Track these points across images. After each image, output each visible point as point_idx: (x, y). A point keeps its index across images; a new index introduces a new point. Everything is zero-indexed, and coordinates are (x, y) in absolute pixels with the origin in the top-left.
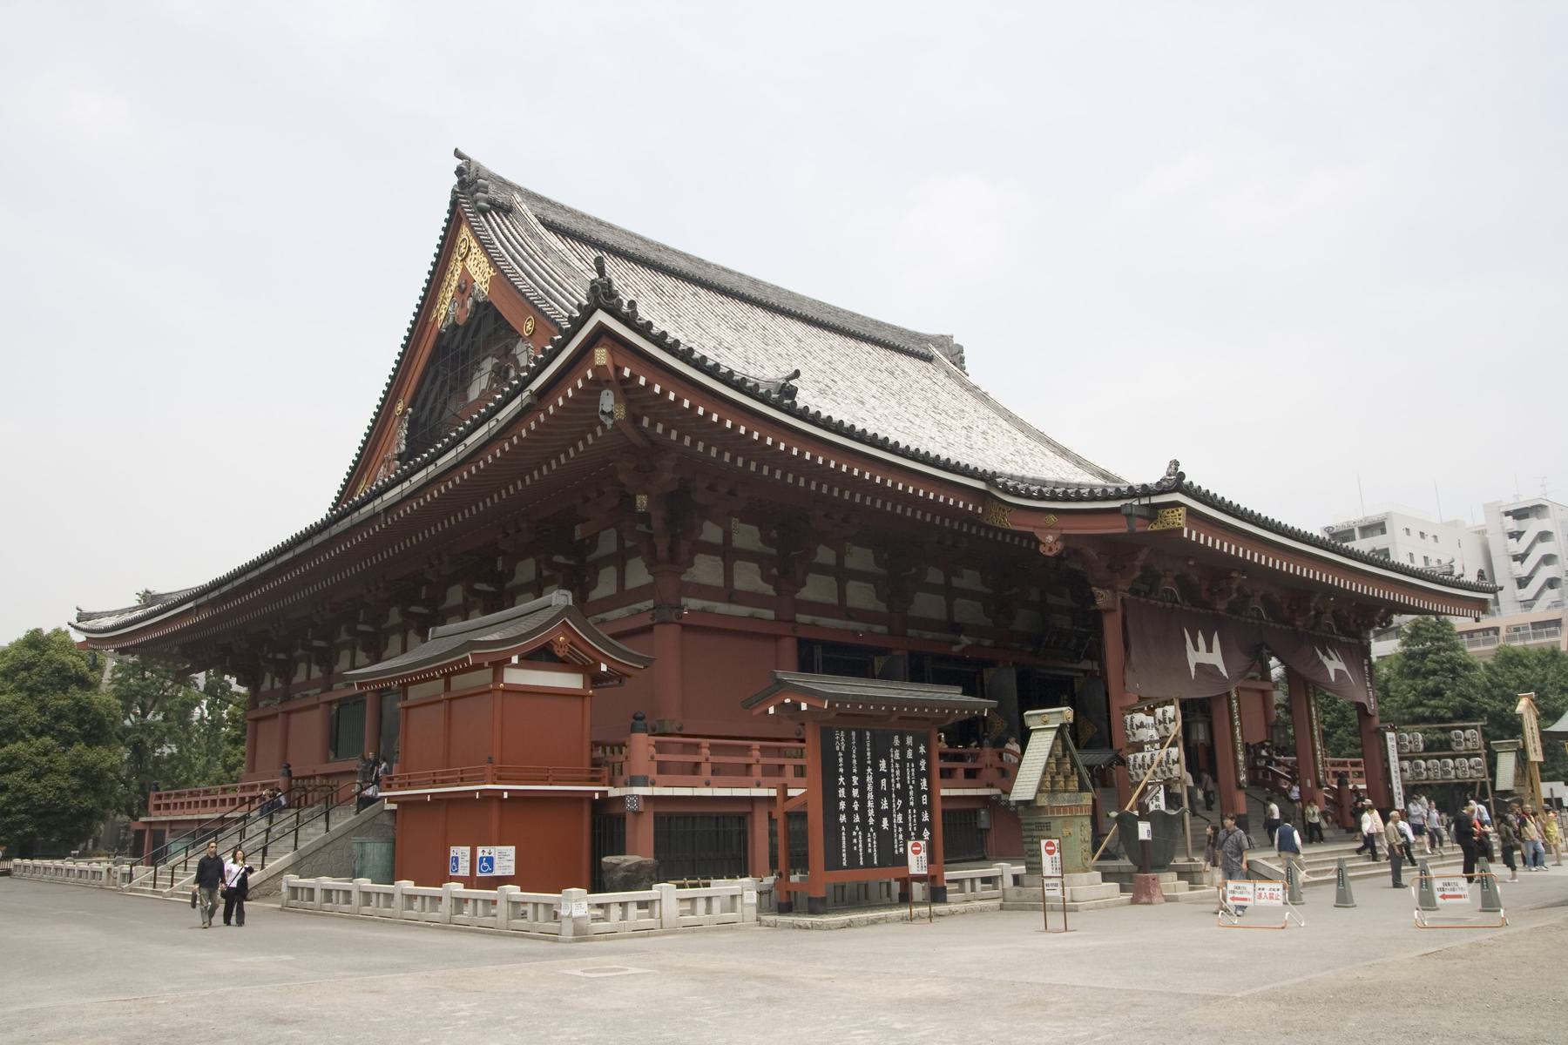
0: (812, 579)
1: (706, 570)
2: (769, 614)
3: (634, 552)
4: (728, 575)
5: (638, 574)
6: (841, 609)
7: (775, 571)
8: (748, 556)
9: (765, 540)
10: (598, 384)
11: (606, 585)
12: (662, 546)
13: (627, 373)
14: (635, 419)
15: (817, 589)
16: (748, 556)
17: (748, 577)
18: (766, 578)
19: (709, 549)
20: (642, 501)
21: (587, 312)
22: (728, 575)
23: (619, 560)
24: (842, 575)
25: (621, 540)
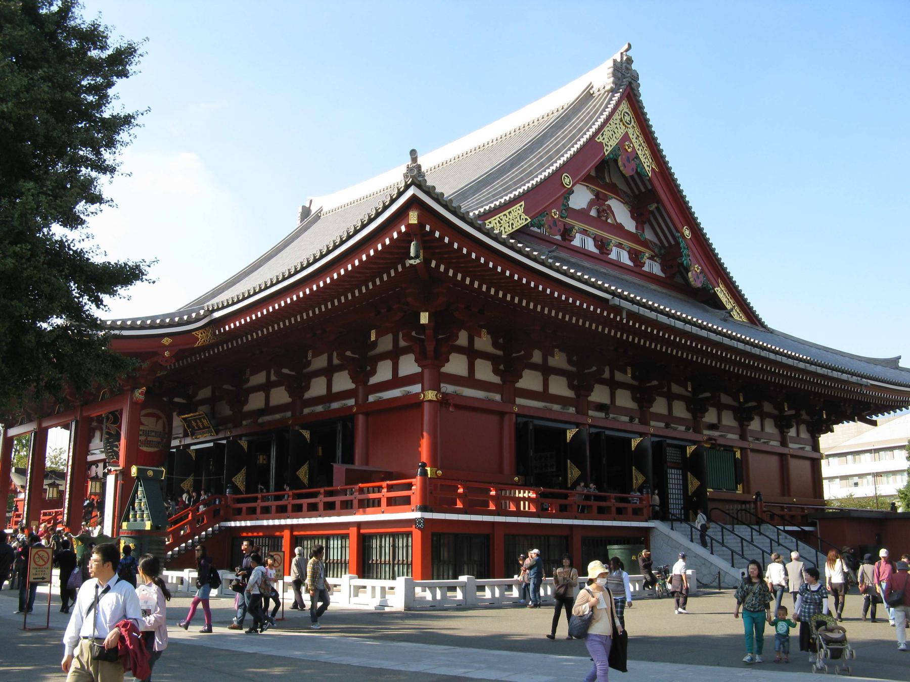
0: (527, 373)
1: (456, 365)
2: (498, 397)
3: (405, 351)
4: (471, 368)
5: (409, 366)
6: (544, 395)
7: (502, 367)
8: (485, 356)
9: (495, 344)
10: (405, 239)
11: (384, 373)
12: (430, 348)
13: (428, 228)
14: (427, 261)
15: (530, 381)
16: (485, 356)
17: (484, 371)
18: (496, 371)
19: (460, 350)
20: (424, 318)
21: (407, 187)
22: (471, 368)
23: (394, 355)
24: (546, 371)
25: (396, 341)
